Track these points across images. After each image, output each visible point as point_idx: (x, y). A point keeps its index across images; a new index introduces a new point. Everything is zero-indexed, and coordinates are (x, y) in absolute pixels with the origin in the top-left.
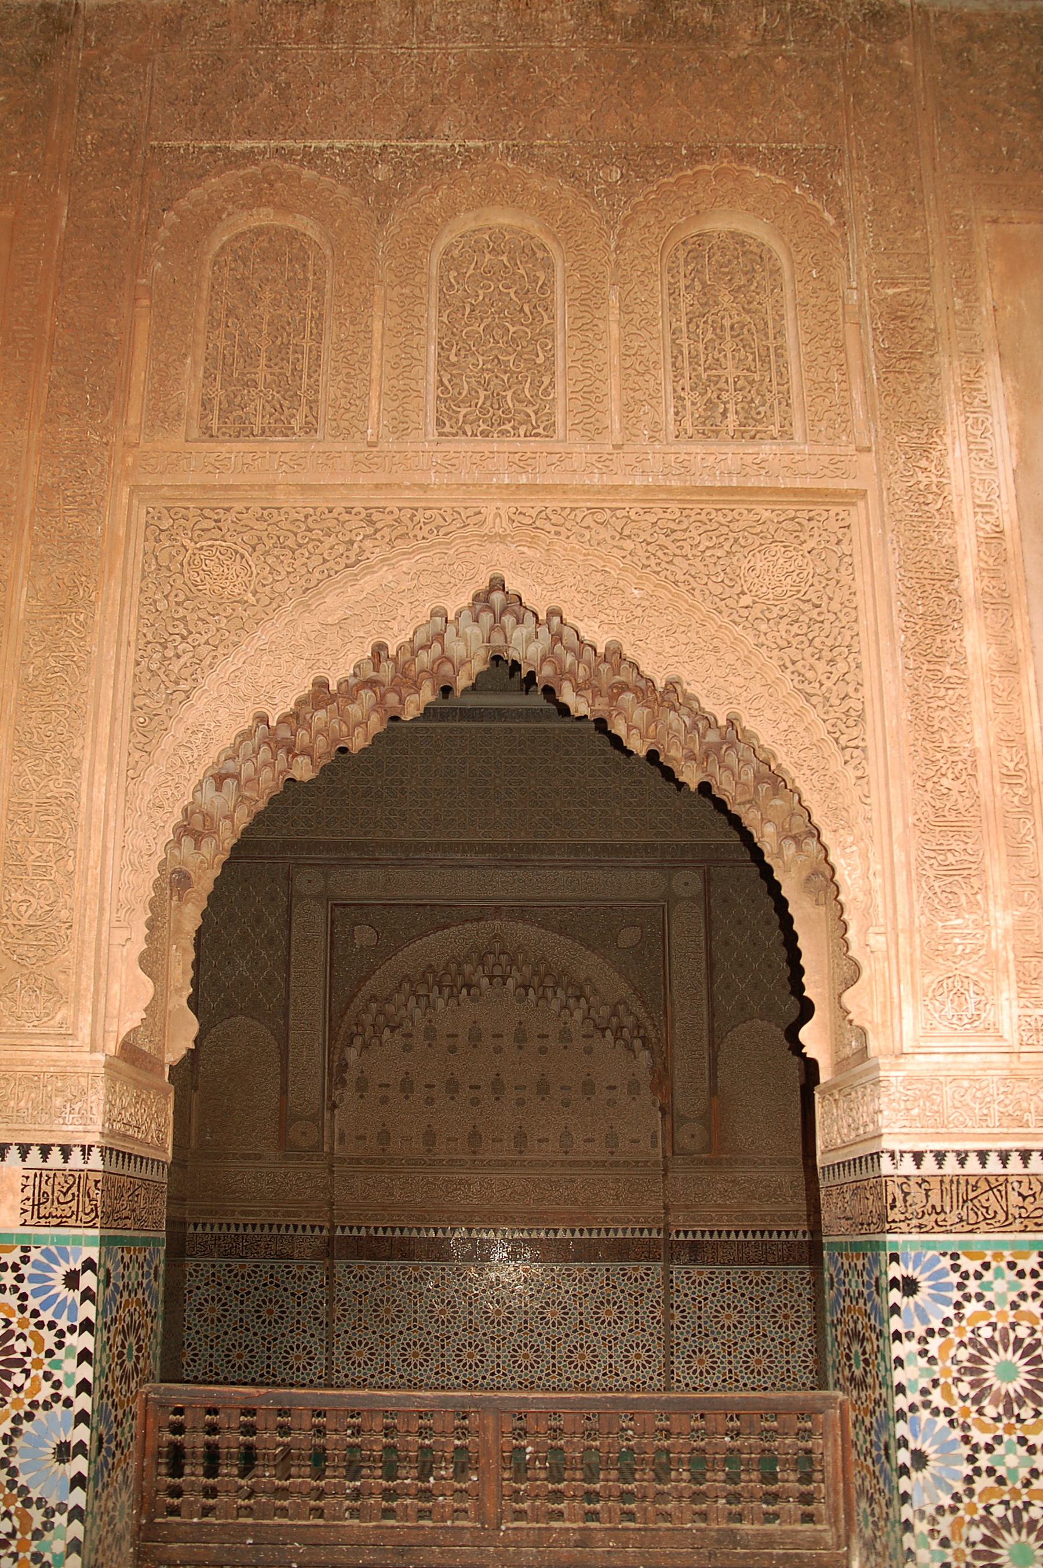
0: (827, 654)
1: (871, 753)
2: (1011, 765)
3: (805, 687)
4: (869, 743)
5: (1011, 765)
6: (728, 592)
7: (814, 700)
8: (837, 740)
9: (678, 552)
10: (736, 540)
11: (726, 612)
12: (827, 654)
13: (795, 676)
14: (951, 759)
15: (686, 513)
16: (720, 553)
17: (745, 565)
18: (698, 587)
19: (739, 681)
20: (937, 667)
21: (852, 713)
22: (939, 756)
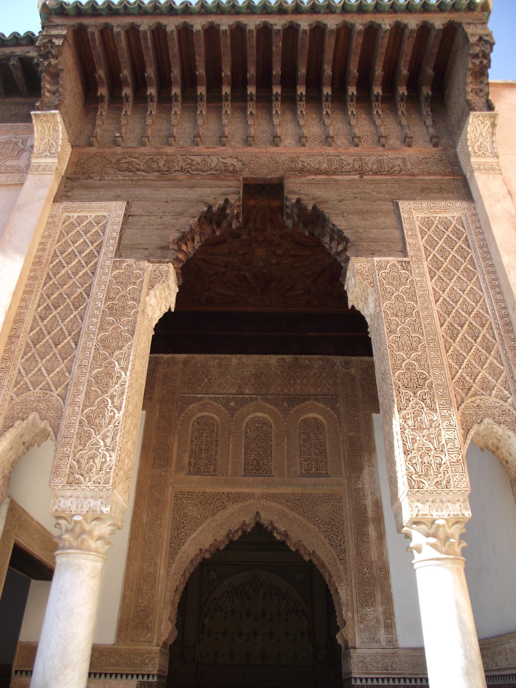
0: (336, 534)
2: (381, 565)
5: (381, 565)
11: (312, 522)
16: (310, 506)
17: (317, 509)
19: (315, 540)
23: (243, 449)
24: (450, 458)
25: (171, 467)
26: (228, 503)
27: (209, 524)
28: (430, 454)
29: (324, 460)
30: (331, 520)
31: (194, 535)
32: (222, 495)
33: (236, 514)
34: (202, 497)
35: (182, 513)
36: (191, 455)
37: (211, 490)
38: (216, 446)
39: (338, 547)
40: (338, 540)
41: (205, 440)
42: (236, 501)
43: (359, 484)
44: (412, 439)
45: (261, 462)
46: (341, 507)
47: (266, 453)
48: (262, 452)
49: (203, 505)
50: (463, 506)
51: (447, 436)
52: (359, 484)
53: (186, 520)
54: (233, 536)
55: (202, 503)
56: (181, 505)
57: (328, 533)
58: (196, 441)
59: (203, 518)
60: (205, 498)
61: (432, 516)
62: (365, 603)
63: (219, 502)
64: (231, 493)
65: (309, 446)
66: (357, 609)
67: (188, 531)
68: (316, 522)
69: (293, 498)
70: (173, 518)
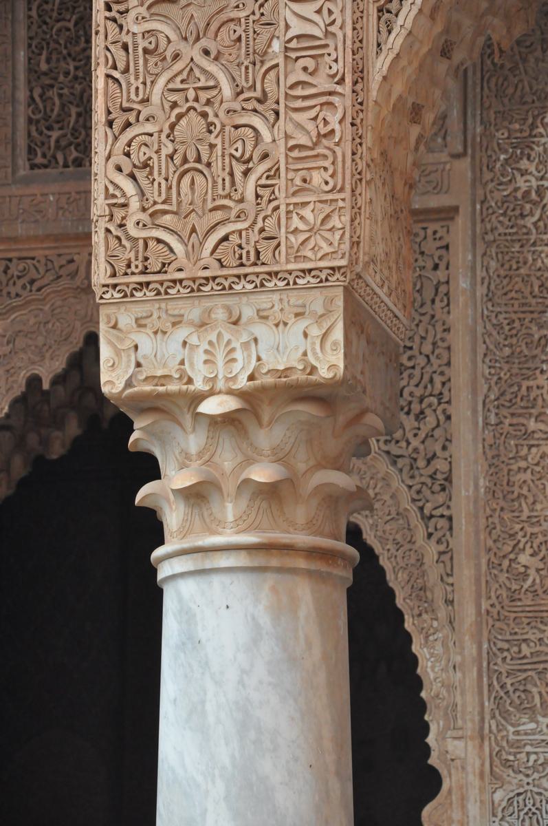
0: (416, 407)
4: (453, 512)
7: (400, 462)
8: (421, 509)
12: (416, 407)
14: (529, 530)
20: (522, 420)
21: (439, 476)
22: (517, 527)
24: (290, 128)
28: (211, 118)
39: (421, 463)
40: (422, 435)
43: (524, 173)
44: (146, 51)
46: (443, 289)
50: (315, 332)
51: (297, 28)
52: (524, 173)
54: (45, 442)
61: (190, 381)
62: (515, 697)
66: (482, 720)
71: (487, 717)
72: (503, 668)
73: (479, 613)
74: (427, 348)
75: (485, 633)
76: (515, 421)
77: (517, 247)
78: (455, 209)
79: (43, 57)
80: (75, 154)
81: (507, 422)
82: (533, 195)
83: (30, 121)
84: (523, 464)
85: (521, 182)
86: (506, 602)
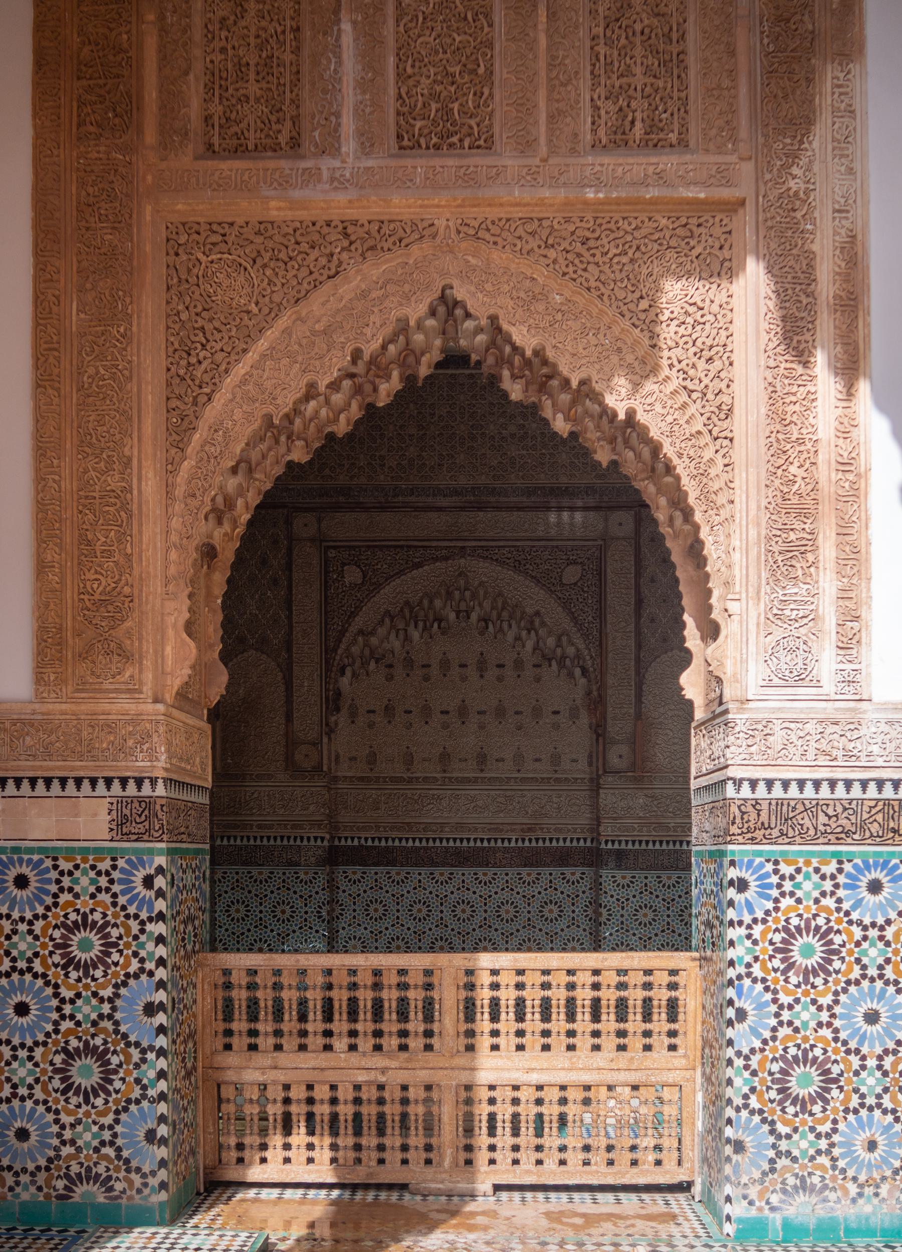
1: (735, 441)
2: (845, 454)
3: (688, 383)
5: (845, 454)
6: (630, 297)
9: (591, 259)
10: (638, 248)
11: (628, 315)
13: (681, 374)
15: (599, 221)
16: (625, 259)
17: (645, 271)
18: (607, 293)
21: (724, 407)
23: (391, 60)
25: (140, 131)
26: (345, 256)
27: (287, 332)
29: (676, 95)
30: (692, 309)
31: (241, 369)
32: (326, 230)
33: (374, 295)
34: (259, 240)
35: (197, 296)
36: (209, 88)
37: (289, 215)
38: (297, 51)
39: (710, 396)
40: (711, 375)
41: (253, 30)
42: (372, 248)
45: (456, 106)
46: (727, 264)
47: (474, 72)
48: (457, 69)
49: (265, 266)
53: (211, 320)
55: (259, 262)
56: (189, 271)
57: (678, 352)
58: (224, 34)
59: (266, 310)
60: (270, 244)
63: (315, 254)
64: (355, 223)
65: (623, 41)
67: (220, 356)
68: (642, 316)
69: (564, 234)
70: (168, 316)
71: (764, 582)
72: (776, 548)
73: (759, 507)
74: (715, 308)
75: (764, 524)
76: (788, 365)
77: (789, 233)
78: (742, 203)
79: (410, 62)
80: (435, 140)
81: (783, 365)
82: (802, 195)
83: (398, 113)
84: (794, 399)
85: (791, 183)
86: (780, 501)
